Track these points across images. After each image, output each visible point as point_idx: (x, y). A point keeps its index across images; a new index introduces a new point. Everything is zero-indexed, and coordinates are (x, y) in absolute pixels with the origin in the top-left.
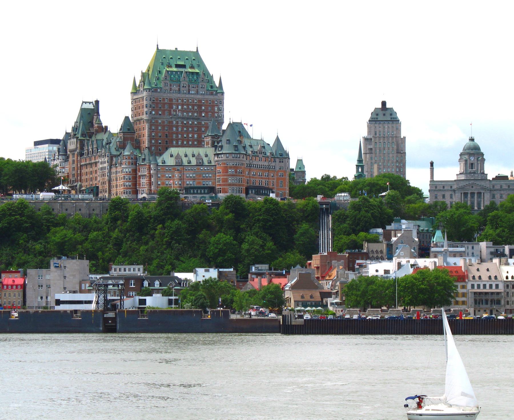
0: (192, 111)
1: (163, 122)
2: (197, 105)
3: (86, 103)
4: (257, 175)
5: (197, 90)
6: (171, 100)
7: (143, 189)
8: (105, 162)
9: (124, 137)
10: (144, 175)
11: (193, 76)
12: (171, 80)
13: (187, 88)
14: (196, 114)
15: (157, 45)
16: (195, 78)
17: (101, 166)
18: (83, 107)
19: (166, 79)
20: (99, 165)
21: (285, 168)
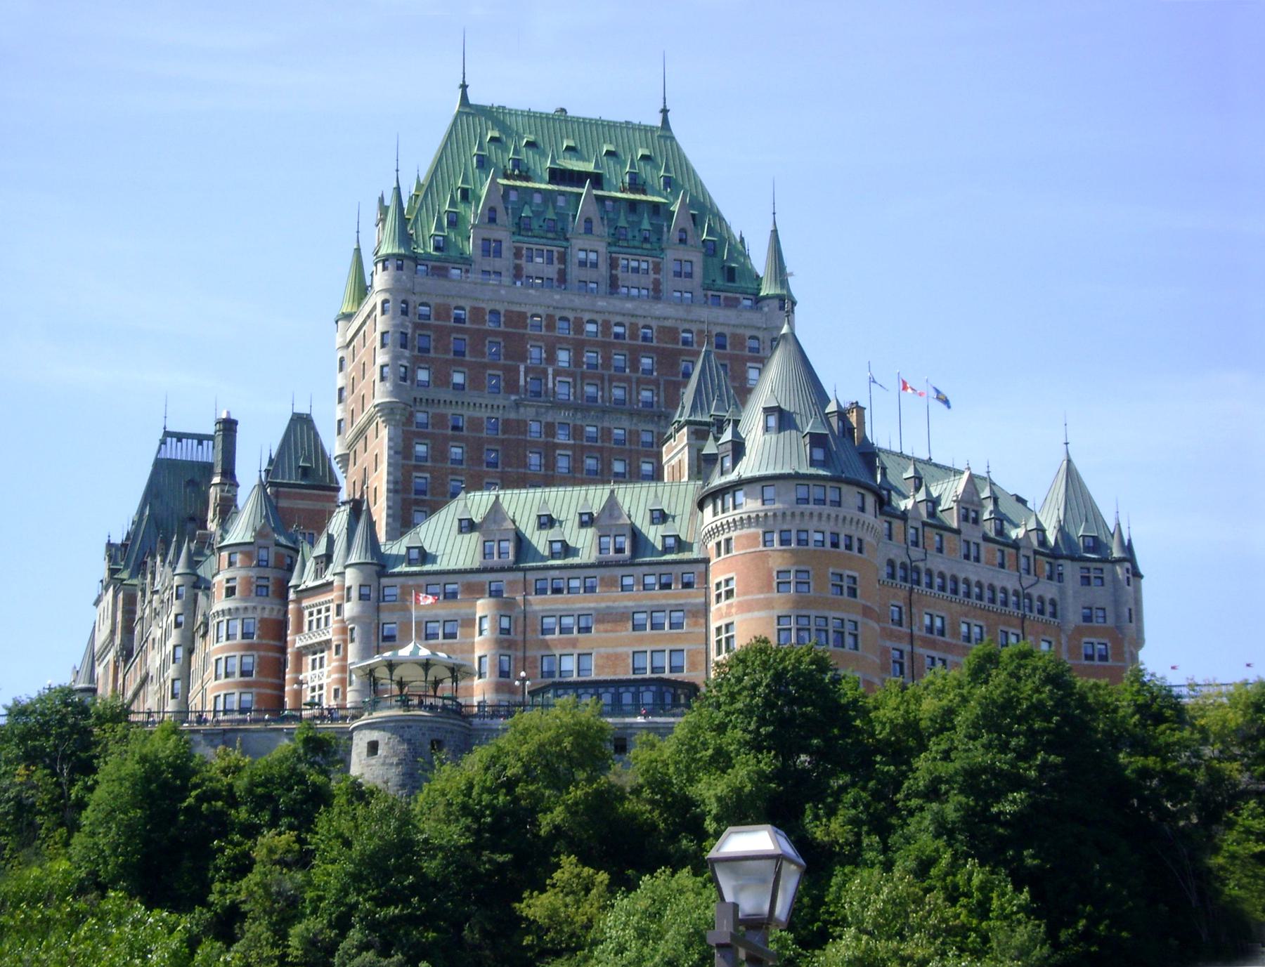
0: (628, 380)
1: (476, 424)
2: (656, 350)
3: (180, 437)
4: (956, 633)
5: (657, 283)
6: (517, 319)
8: (166, 635)
11: (635, 218)
12: (521, 227)
13: (603, 268)
14: (646, 395)
15: (464, 87)
16: (646, 225)
18: (162, 456)
19: (492, 220)
21: (1118, 617)
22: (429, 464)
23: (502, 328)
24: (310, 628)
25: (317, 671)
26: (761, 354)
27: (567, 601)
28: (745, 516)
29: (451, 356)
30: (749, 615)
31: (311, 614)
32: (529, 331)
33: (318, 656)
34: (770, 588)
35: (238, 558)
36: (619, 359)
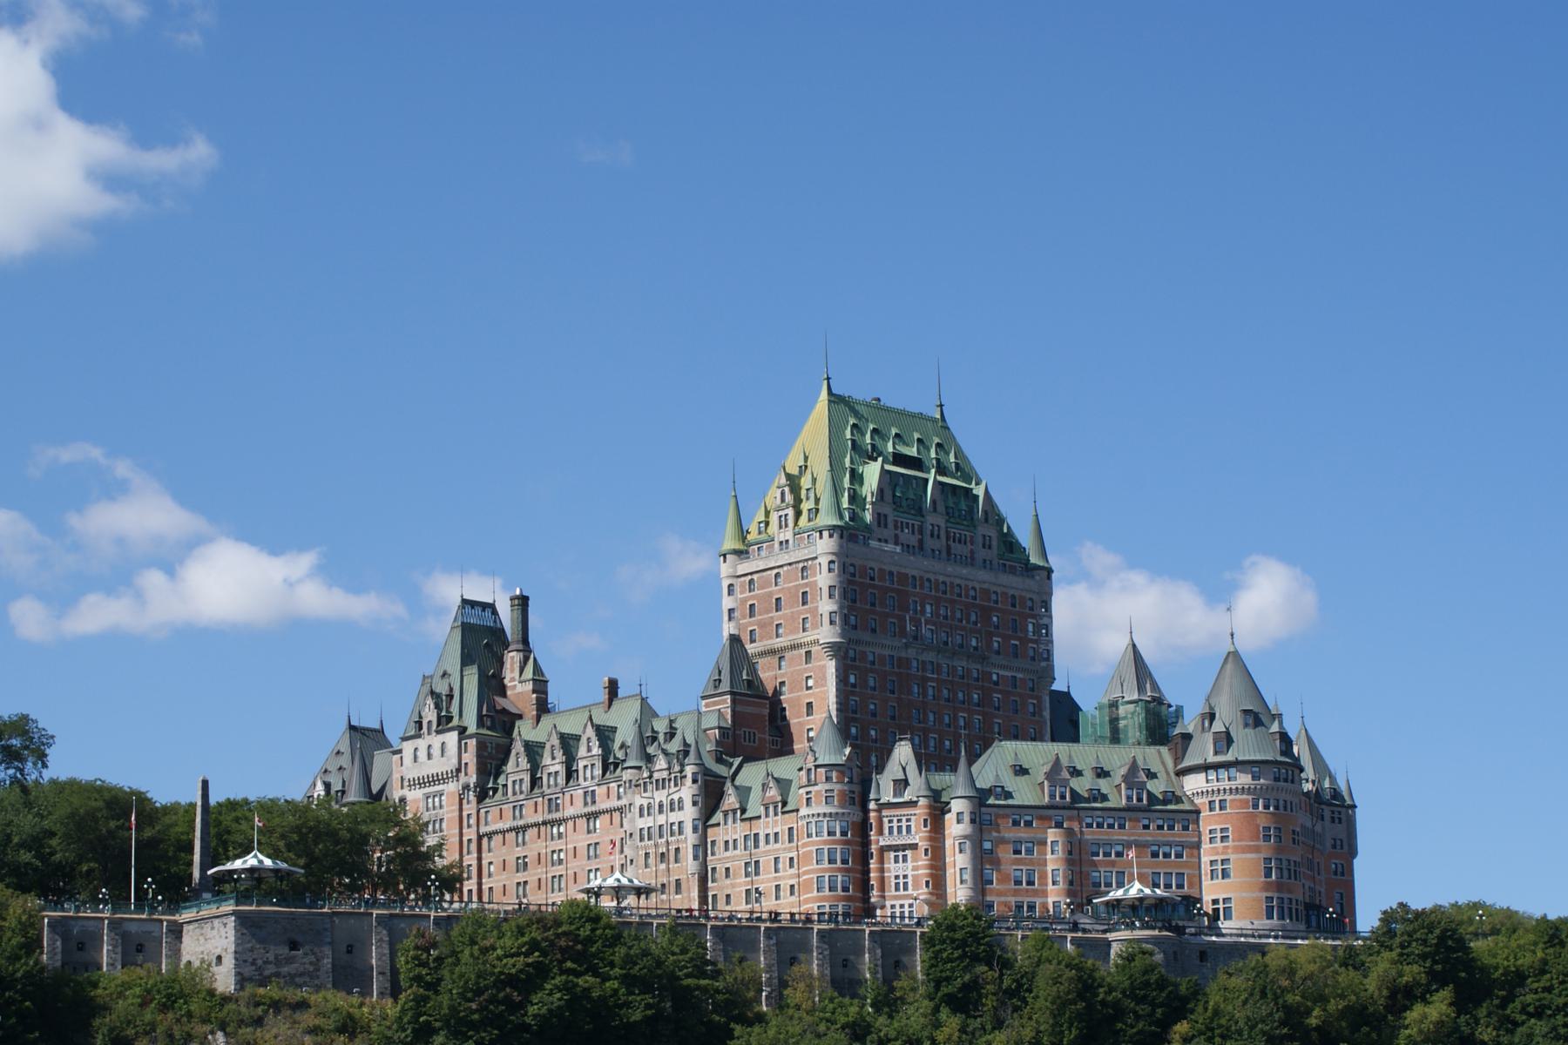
0: (963, 629)
6: (903, 578)
7: (897, 903)
9: (733, 711)
10: (904, 847)
17: (645, 822)
20: (632, 821)
22: (857, 690)
23: (895, 586)
24: (891, 832)
25: (901, 864)
26: (1035, 612)
27: (1107, 834)
28: (1240, 787)
29: (868, 607)
30: (1244, 856)
31: (890, 821)
32: (910, 589)
33: (900, 854)
34: (1258, 839)
35: (834, 774)
36: (958, 615)
